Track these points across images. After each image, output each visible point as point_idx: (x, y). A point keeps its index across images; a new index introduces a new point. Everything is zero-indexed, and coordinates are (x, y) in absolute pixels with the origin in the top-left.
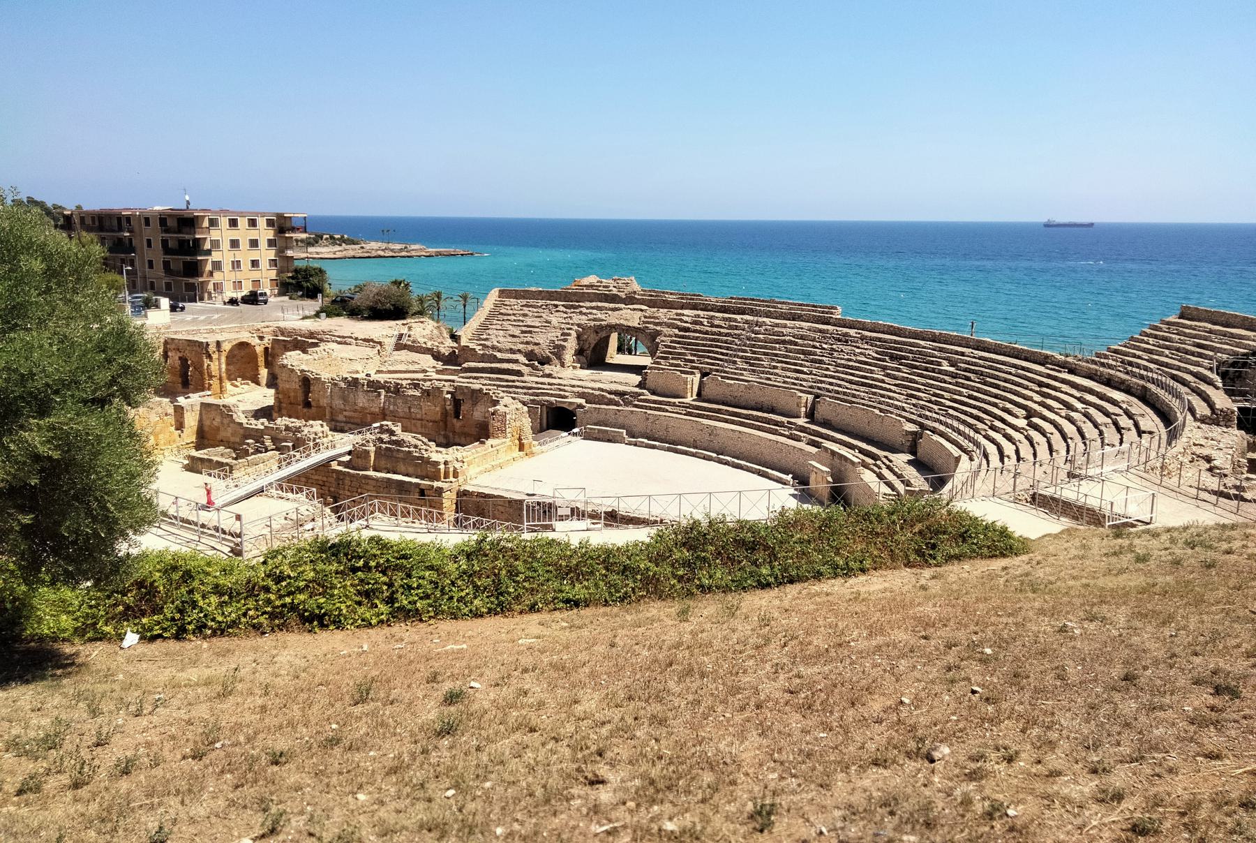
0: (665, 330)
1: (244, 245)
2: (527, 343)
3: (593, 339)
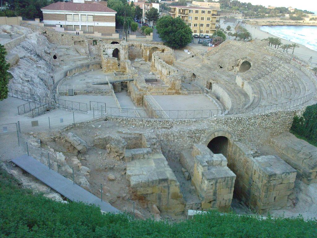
1: (199, 19)
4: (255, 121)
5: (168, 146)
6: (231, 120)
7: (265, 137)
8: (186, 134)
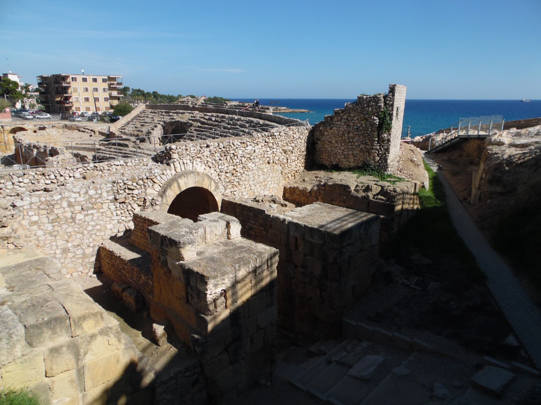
0: (195, 124)
2: (138, 131)
3: (170, 129)
4: (253, 149)
5: (58, 238)
6: (208, 149)
7: (275, 184)
8: (105, 194)
